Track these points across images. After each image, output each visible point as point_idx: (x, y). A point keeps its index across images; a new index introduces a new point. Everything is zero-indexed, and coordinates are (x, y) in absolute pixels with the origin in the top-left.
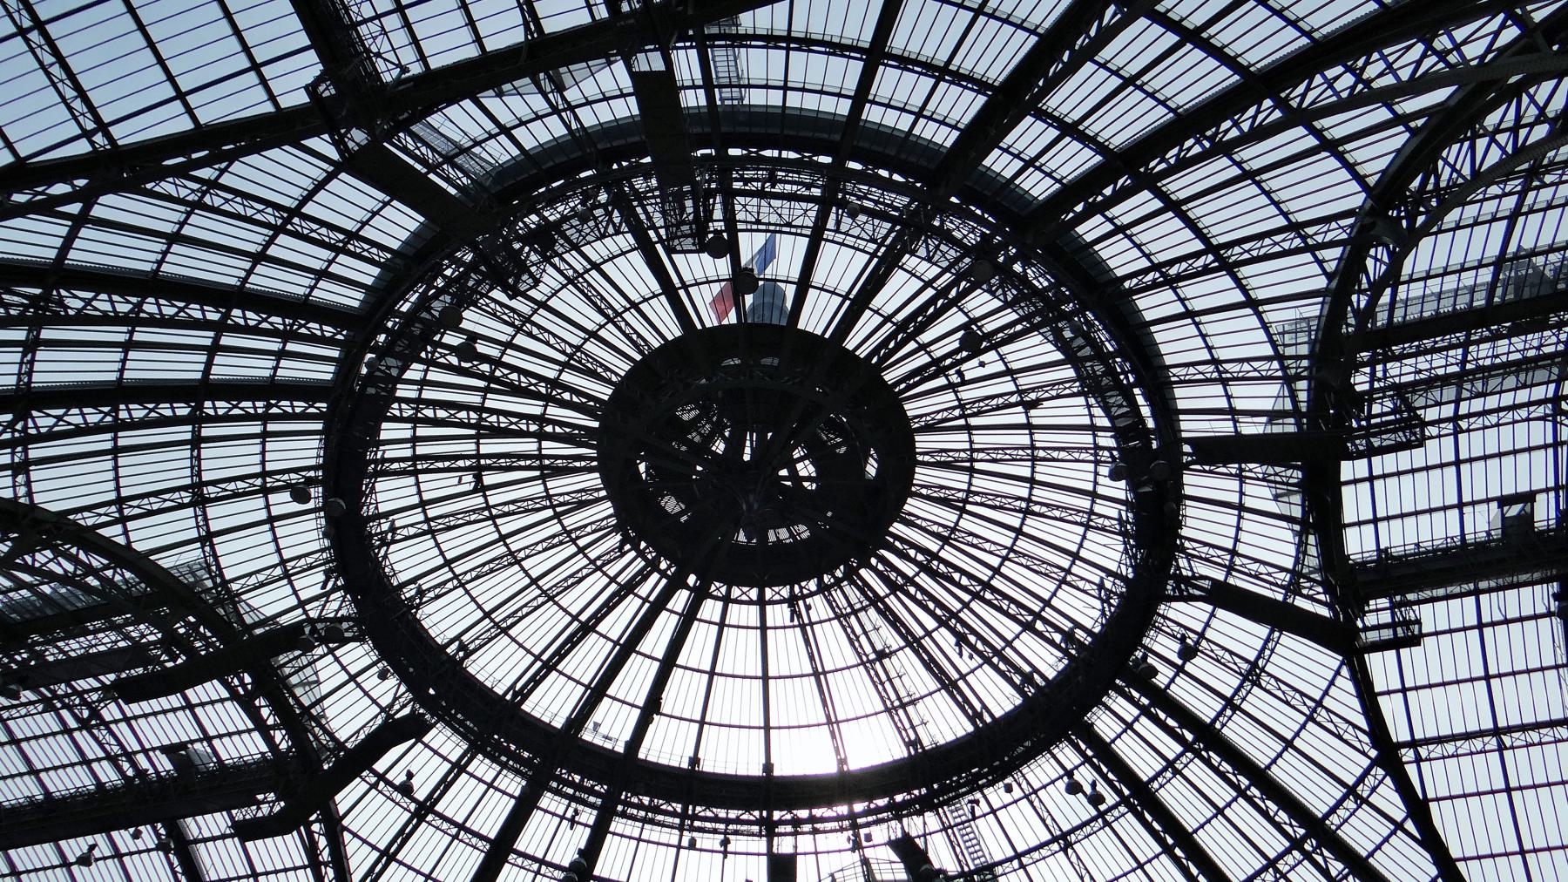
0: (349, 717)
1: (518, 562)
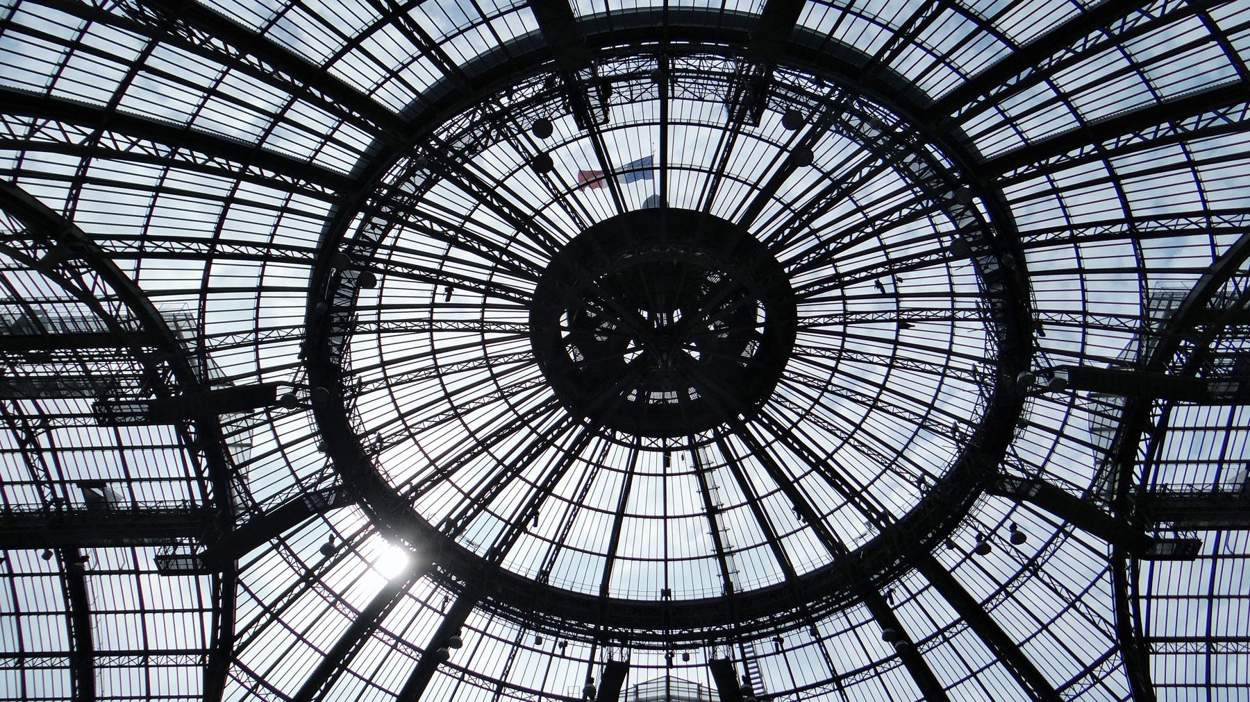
0: (267, 484)
1: (440, 376)
